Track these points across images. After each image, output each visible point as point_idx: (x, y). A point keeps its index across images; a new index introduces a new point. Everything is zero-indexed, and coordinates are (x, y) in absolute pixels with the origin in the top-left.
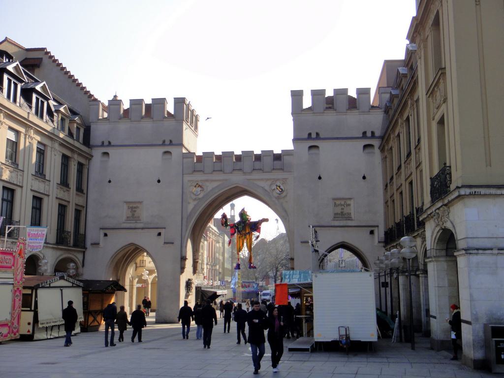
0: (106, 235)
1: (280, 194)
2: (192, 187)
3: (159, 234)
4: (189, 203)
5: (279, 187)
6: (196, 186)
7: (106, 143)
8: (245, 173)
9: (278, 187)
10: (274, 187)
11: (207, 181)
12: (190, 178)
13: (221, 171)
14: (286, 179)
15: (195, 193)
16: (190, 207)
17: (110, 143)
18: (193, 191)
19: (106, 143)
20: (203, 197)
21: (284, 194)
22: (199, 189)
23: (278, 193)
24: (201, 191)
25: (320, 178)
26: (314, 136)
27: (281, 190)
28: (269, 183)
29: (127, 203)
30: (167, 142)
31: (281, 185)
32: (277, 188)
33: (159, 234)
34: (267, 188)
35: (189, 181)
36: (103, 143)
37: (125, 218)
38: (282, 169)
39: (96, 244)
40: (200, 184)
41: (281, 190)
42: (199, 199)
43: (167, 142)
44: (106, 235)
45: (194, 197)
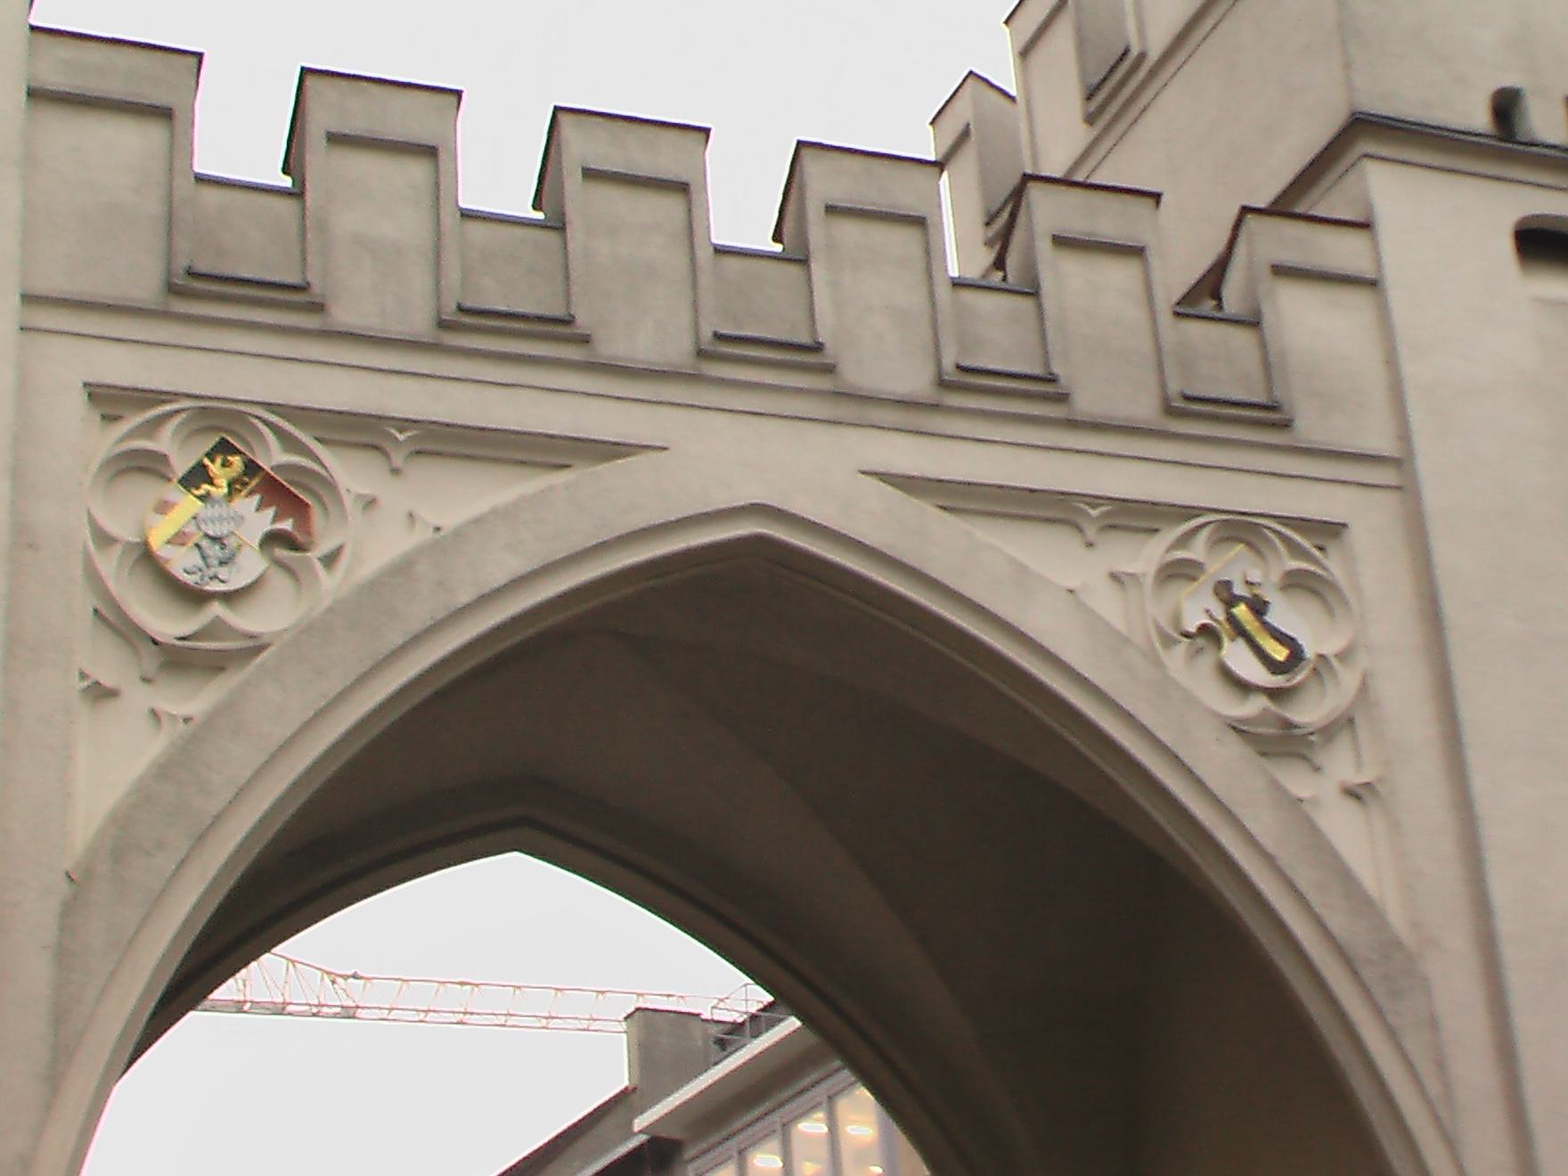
1: (1274, 694)
2: (146, 491)
4: (100, 693)
5: (1259, 608)
6: (197, 477)
8: (858, 404)
9: (1241, 611)
10: (1198, 608)
11: (362, 431)
12: (124, 368)
14: (1329, 531)
15: (182, 562)
16: (110, 758)
18: (157, 542)
20: (312, 631)
21: (1308, 713)
23: (1244, 687)
24: (273, 539)
27: (1280, 653)
31: (1269, 594)
32: (1240, 631)
34: (1108, 604)
35: (108, 400)
38: (1267, 416)
40: (273, 456)
41: (1280, 653)
42: (255, 647)
45: (169, 624)
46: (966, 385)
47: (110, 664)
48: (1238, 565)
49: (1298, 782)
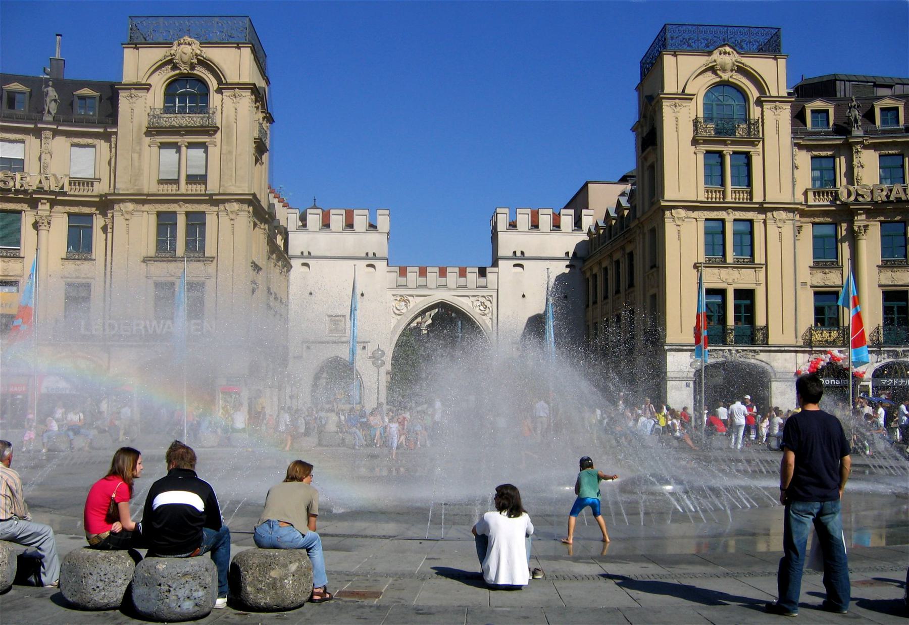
0: (308, 348)
3: (364, 348)
7: (306, 254)
13: (426, 286)
17: (309, 253)
19: (306, 254)
22: (403, 303)
25: (524, 296)
26: (519, 254)
28: (473, 299)
29: (329, 316)
30: (371, 255)
33: (364, 348)
36: (302, 253)
37: (327, 332)
38: (486, 287)
39: (299, 357)
43: (371, 255)
44: (308, 348)
46: (459, 287)
47: (394, 315)
48: (483, 300)
49: (484, 317)
